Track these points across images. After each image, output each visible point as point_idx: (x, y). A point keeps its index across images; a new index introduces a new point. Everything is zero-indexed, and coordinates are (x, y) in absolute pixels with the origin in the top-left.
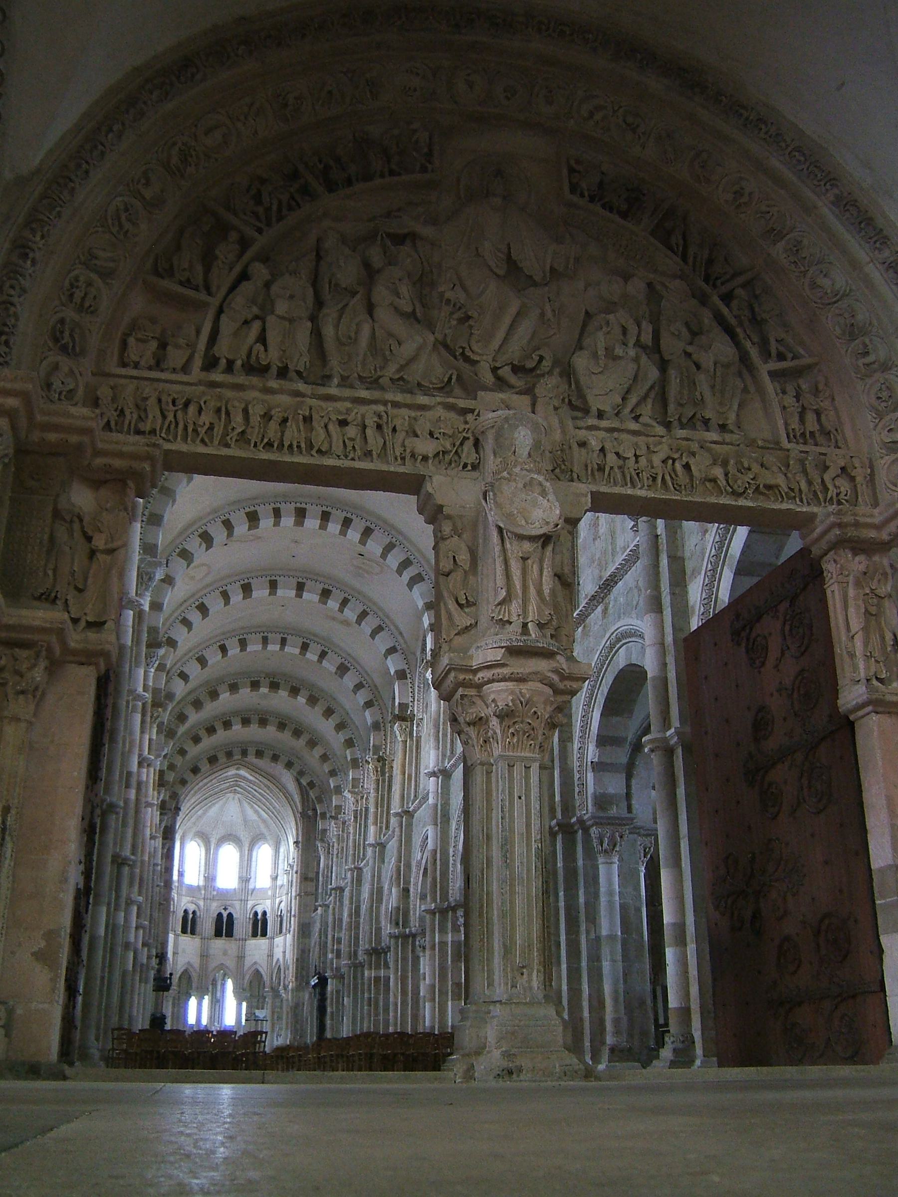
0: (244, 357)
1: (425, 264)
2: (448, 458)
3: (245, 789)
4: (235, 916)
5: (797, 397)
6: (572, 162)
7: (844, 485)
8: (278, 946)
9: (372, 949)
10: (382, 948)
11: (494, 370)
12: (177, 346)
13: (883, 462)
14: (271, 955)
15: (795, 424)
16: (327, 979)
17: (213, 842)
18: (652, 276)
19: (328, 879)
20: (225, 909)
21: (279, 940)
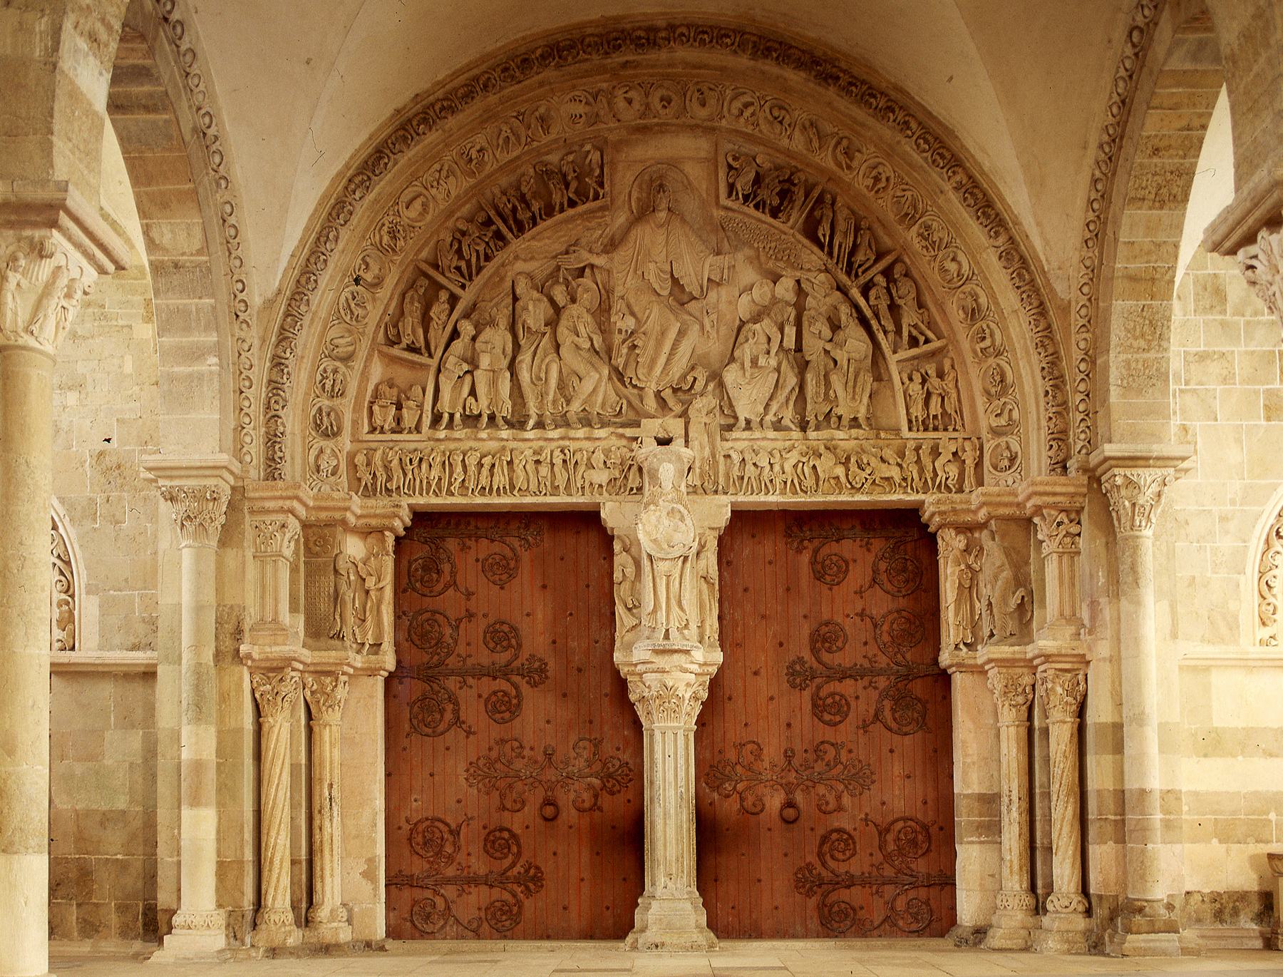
0: (461, 411)
1: (603, 291)
2: (618, 483)
5: (924, 381)
6: (730, 160)
7: (953, 471)
11: (658, 394)
12: (409, 408)
13: (989, 445)
15: (918, 411)
18: (798, 274)
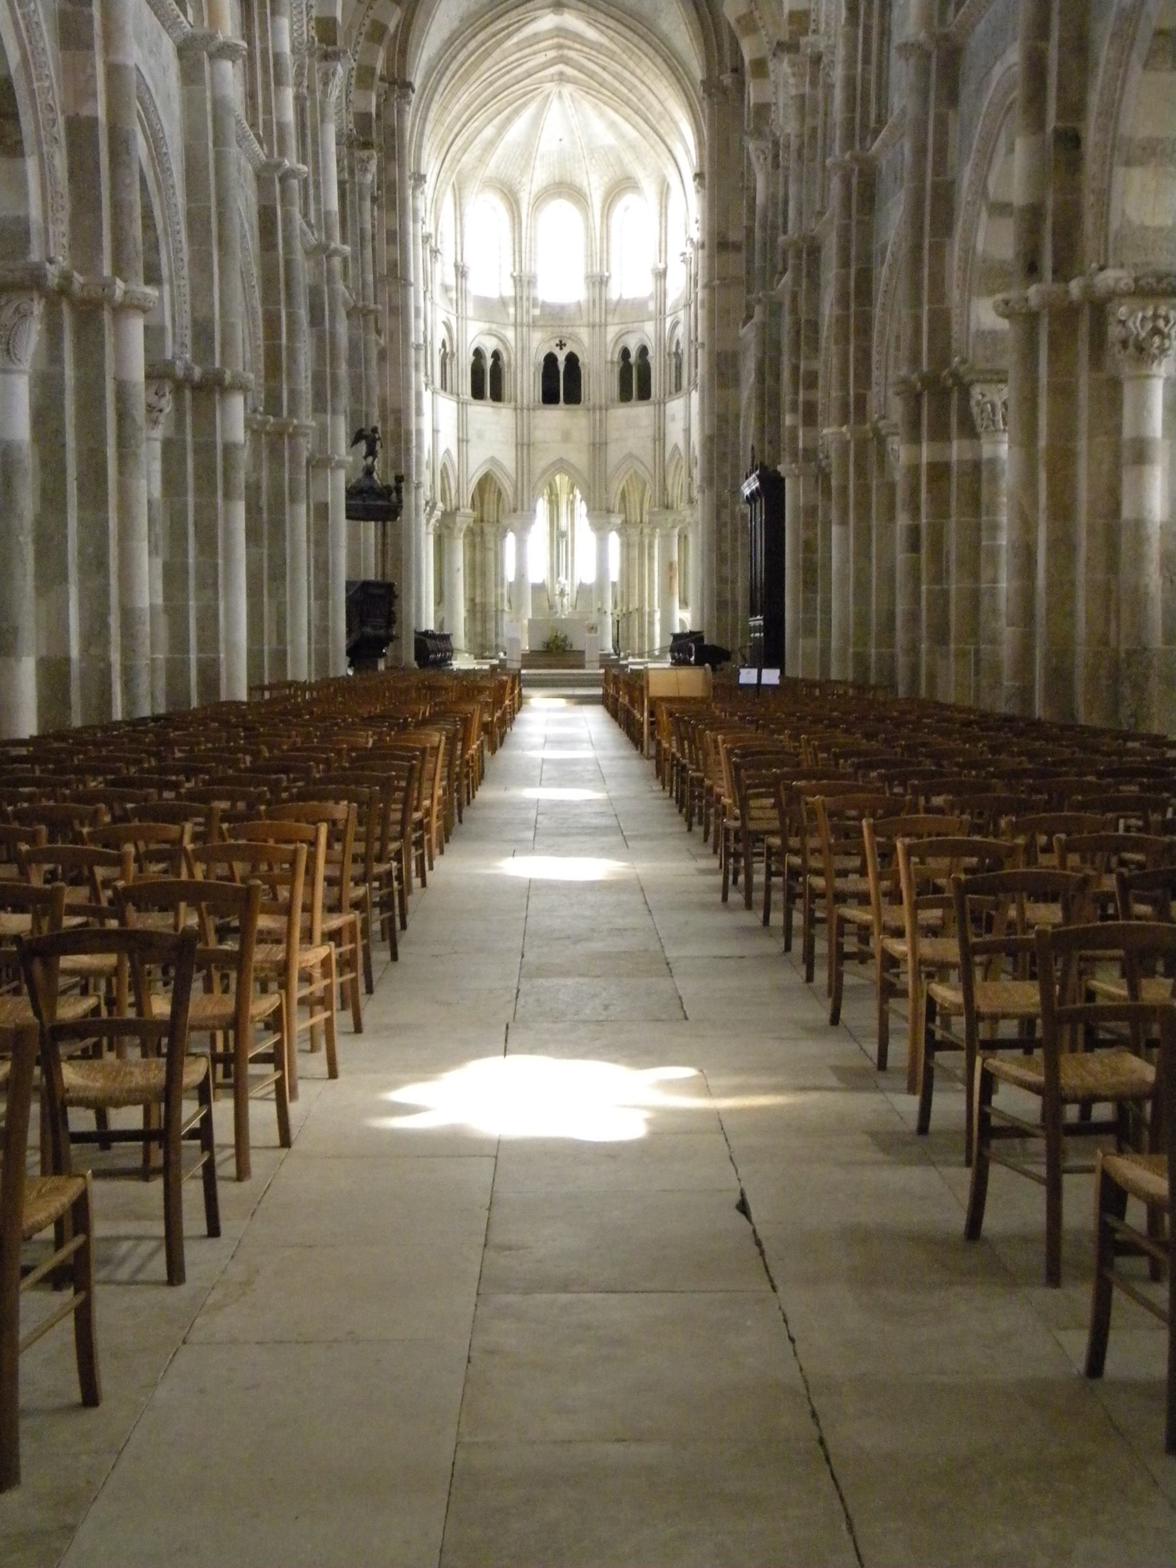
3: (581, 69)
4: (583, 359)
8: (673, 419)
9: (923, 379)
10: (955, 375)
14: (660, 437)
16: (783, 480)
17: (525, 199)
19: (774, 228)
20: (561, 345)
21: (676, 406)
